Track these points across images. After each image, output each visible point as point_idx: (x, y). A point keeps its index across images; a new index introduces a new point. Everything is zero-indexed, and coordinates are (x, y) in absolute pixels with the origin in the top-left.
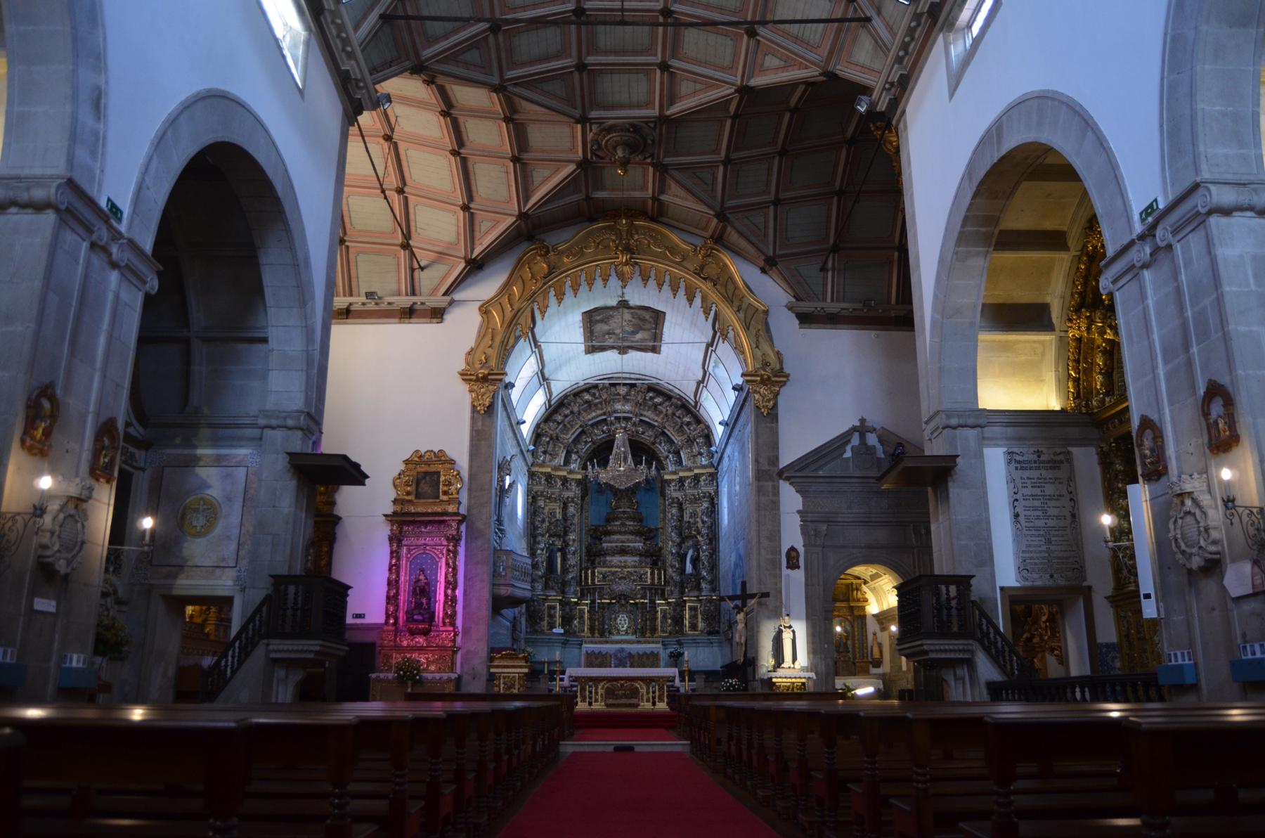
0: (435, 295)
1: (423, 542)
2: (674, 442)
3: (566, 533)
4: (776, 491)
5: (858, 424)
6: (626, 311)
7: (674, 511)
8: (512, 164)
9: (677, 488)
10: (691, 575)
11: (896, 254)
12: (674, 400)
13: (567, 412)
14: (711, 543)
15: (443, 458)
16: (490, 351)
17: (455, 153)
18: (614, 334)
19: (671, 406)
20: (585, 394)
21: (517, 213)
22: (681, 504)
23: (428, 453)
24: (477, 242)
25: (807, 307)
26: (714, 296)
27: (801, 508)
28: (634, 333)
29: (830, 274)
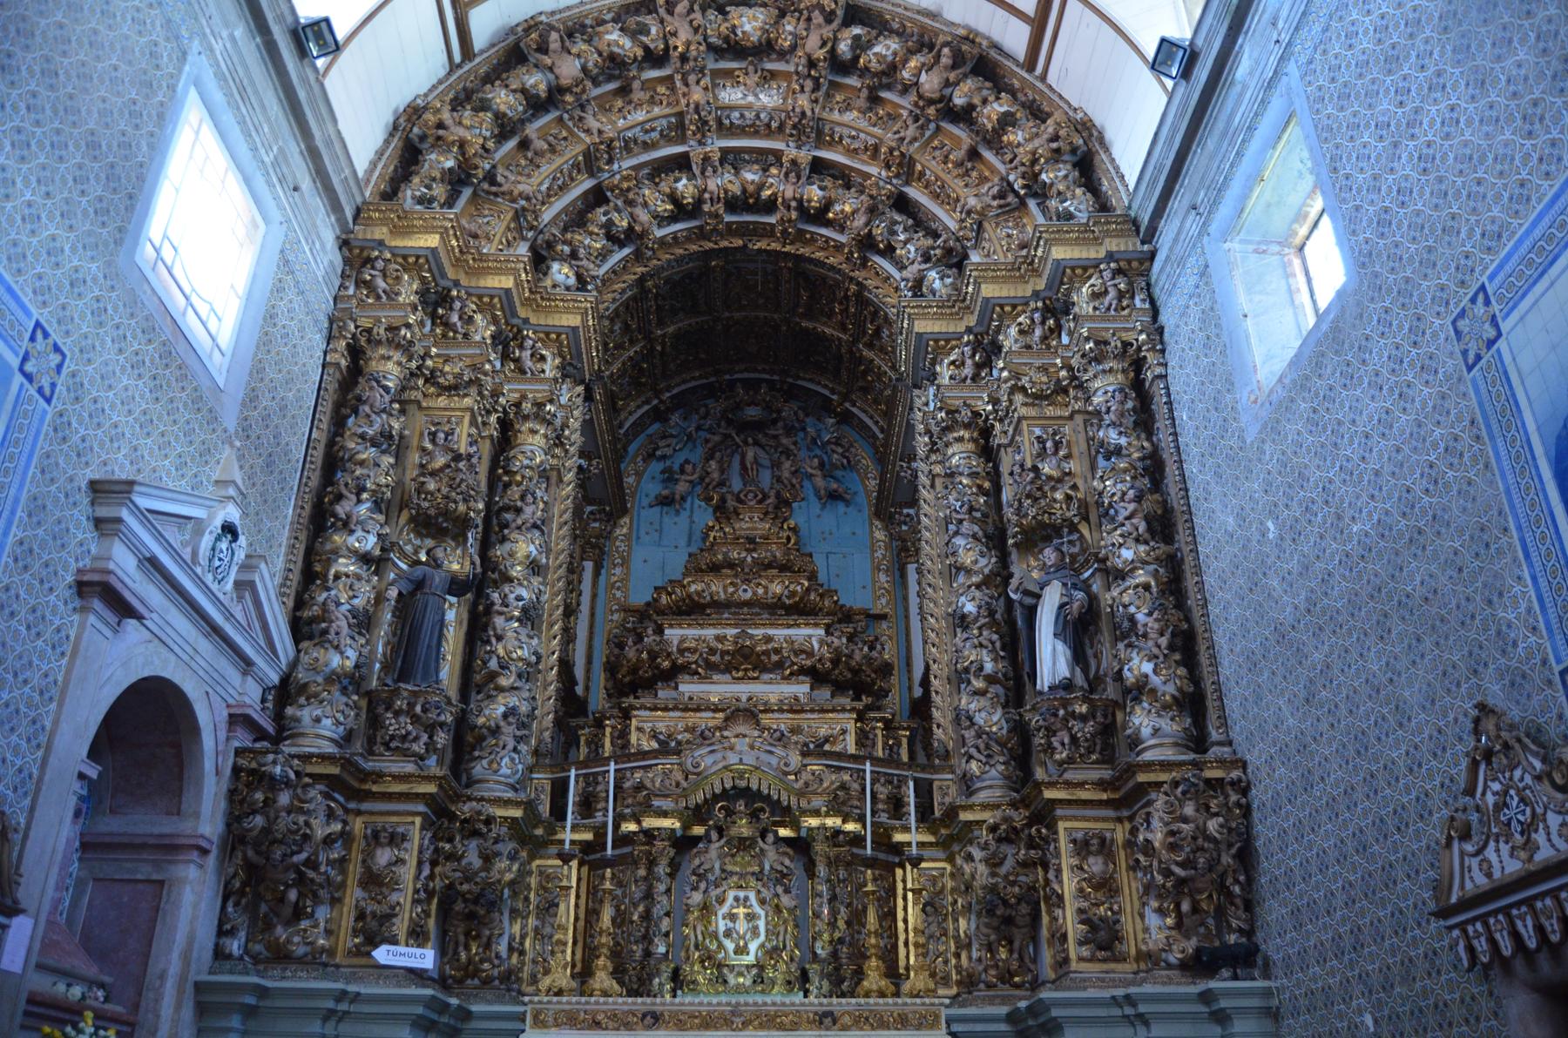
7: (959, 454)
9: (968, 371)
10: (1067, 685)
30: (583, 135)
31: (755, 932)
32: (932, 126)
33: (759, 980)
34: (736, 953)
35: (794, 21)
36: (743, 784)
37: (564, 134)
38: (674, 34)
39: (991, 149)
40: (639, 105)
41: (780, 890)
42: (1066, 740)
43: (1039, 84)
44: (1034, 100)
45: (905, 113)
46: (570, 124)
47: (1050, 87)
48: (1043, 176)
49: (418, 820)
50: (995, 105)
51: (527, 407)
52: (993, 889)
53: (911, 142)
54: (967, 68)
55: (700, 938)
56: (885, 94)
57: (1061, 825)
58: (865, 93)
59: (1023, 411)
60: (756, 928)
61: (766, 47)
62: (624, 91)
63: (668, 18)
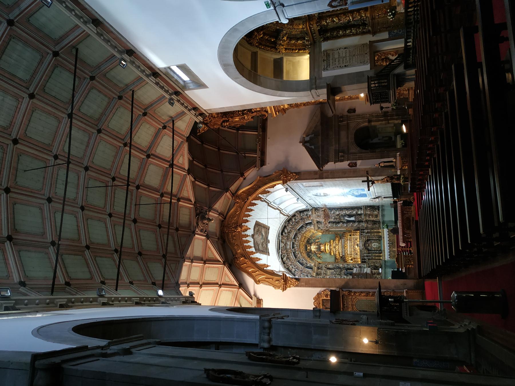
0: (252, 303)
1: (351, 306)
2: (302, 225)
3: (340, 268)
4: (327, 171)
5: (301, 144)
6: (255, 236)
8: (206, 265)
9: (320, 224)
10: (355, 217)
11: (240, 132)
12: (286, 225)
13: (291, 267)
14: (342, 210)
15: (317, 298)
16: (274, 280)
17: (201, 287)
18: (262, 243)
19: (288, 226)
20: (284, 259)
21: (223, 265)
23: (315, 304)
24: (233, 283)
25: (258, 162)
26: (254, 196)
27: (333, 163)
28: (262, 235)
29: (246, 155)
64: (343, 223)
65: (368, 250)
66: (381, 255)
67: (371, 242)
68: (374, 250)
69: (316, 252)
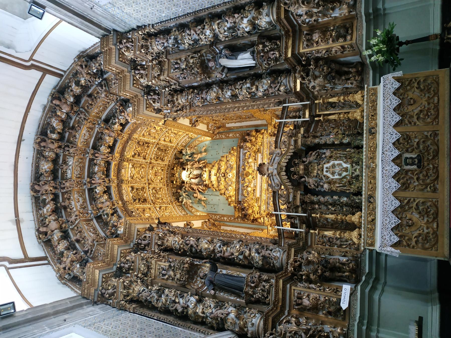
9: (156, 97)
10: (253, 53)
22: (175, 91)
30: (77, 222)
31: (340, 165)
32: (81, 109)
33: (357, 163)
34: (347, 172)
35: (45, 152)
36: (284, 168)
37: (76, 228)
38: (46, 191)
39: (89, 90)
40: (70, 204)
41: (324, 156)
42: (272, 53)
43: (67, 73)
44: (72, 75)
45: (77, 118)
46: (73, 226)
47: (68, 70)
48: (95, 71)
49: (293, 288)
50: (73, 87)
51: (159, 243)
52: (325, 77)
53: (86, 116)
54: (61, 96)
55: (341, 185)
56: (71, 125)
57: (302, 51)
58: (70, 131)
59: (166, 75)
60: (338, 164)
61: (55, 161)
62: (65, 208)
63: (41, 192)
64: (222, 84)
65: (307, 191)
66: (355, 218)
67: (319, 157)
68: (332, 193)
69: (195, 187)
